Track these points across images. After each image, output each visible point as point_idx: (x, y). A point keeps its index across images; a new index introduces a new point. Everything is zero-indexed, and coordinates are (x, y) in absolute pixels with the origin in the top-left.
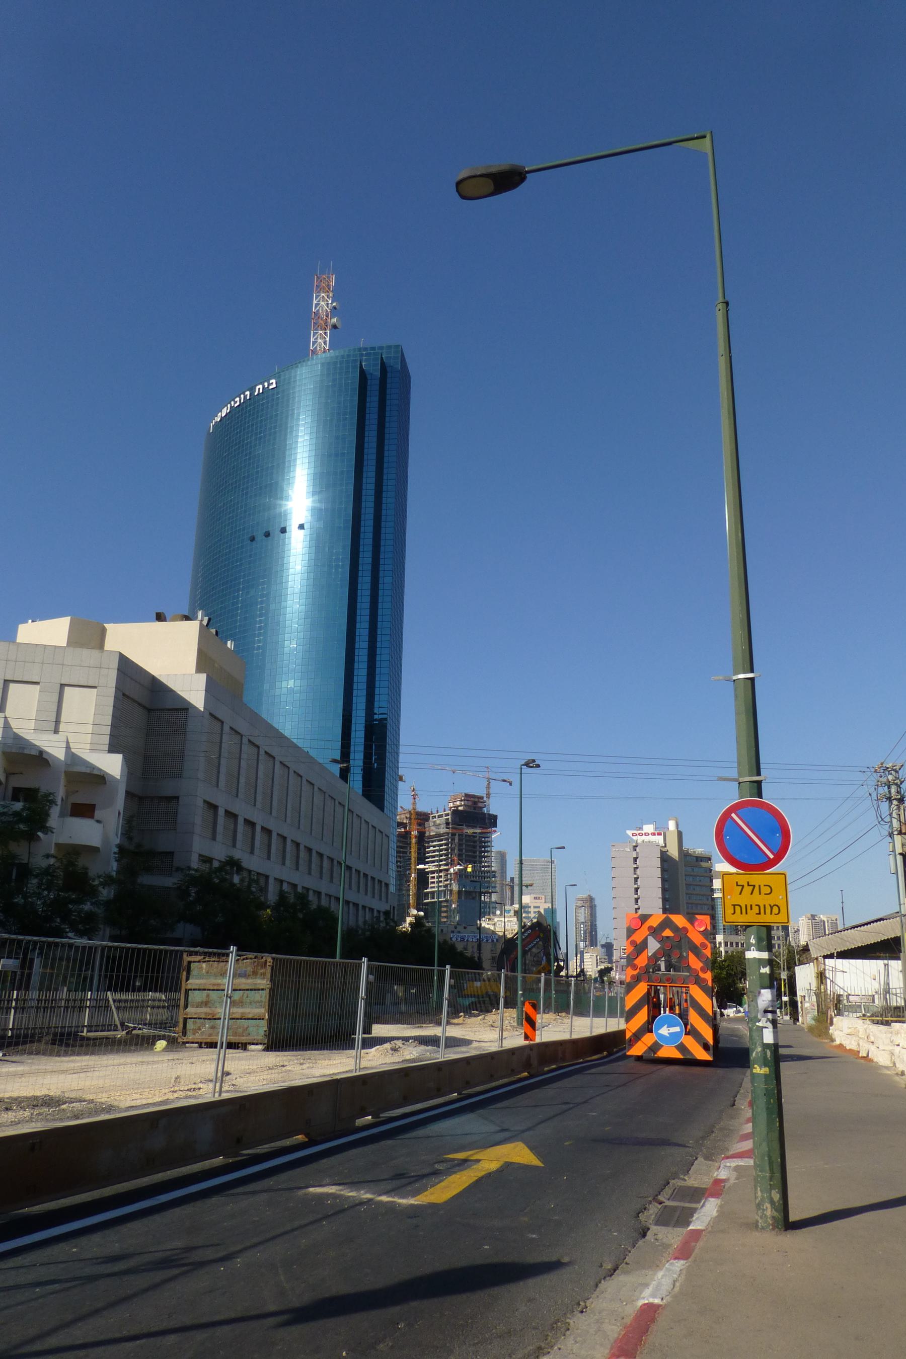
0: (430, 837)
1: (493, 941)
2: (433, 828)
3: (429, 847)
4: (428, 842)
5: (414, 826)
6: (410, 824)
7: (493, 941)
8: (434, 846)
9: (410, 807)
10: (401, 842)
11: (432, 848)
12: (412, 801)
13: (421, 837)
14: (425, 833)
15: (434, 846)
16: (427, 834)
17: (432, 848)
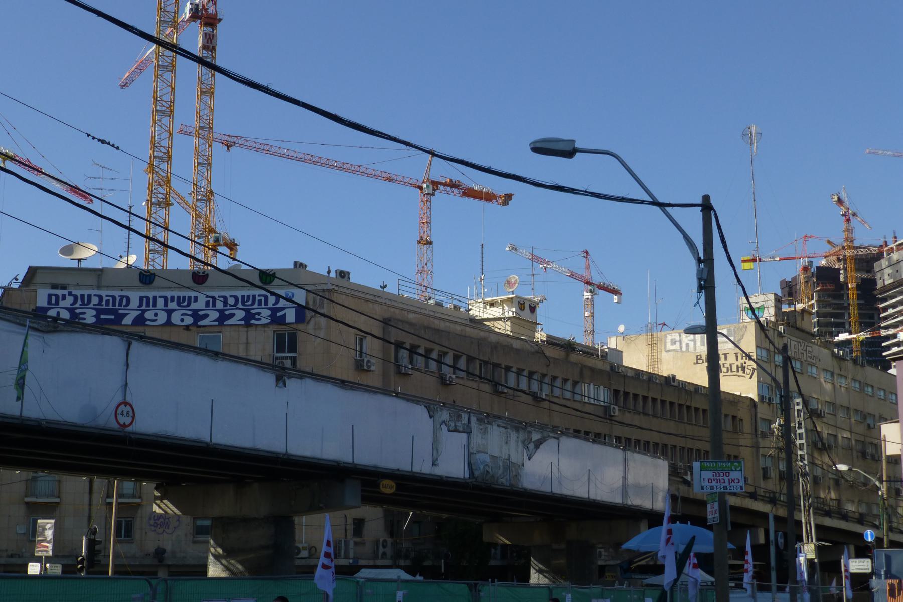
0: (886, 289)
1: (277, 319)
2: (889, 271)
3: (885, 309)
4: (885, 300)
5: (852, 274)
6: (845, 269)
7: (277, 319)
8: (894, 306)
9: (839, 238)
10: (829, 305)
11: (891, 311)
12: (844, 225)
13: (868, 288)
14: (873, 282)
15: (894, 306)
16: (880, 285)
17: (891, 311)
